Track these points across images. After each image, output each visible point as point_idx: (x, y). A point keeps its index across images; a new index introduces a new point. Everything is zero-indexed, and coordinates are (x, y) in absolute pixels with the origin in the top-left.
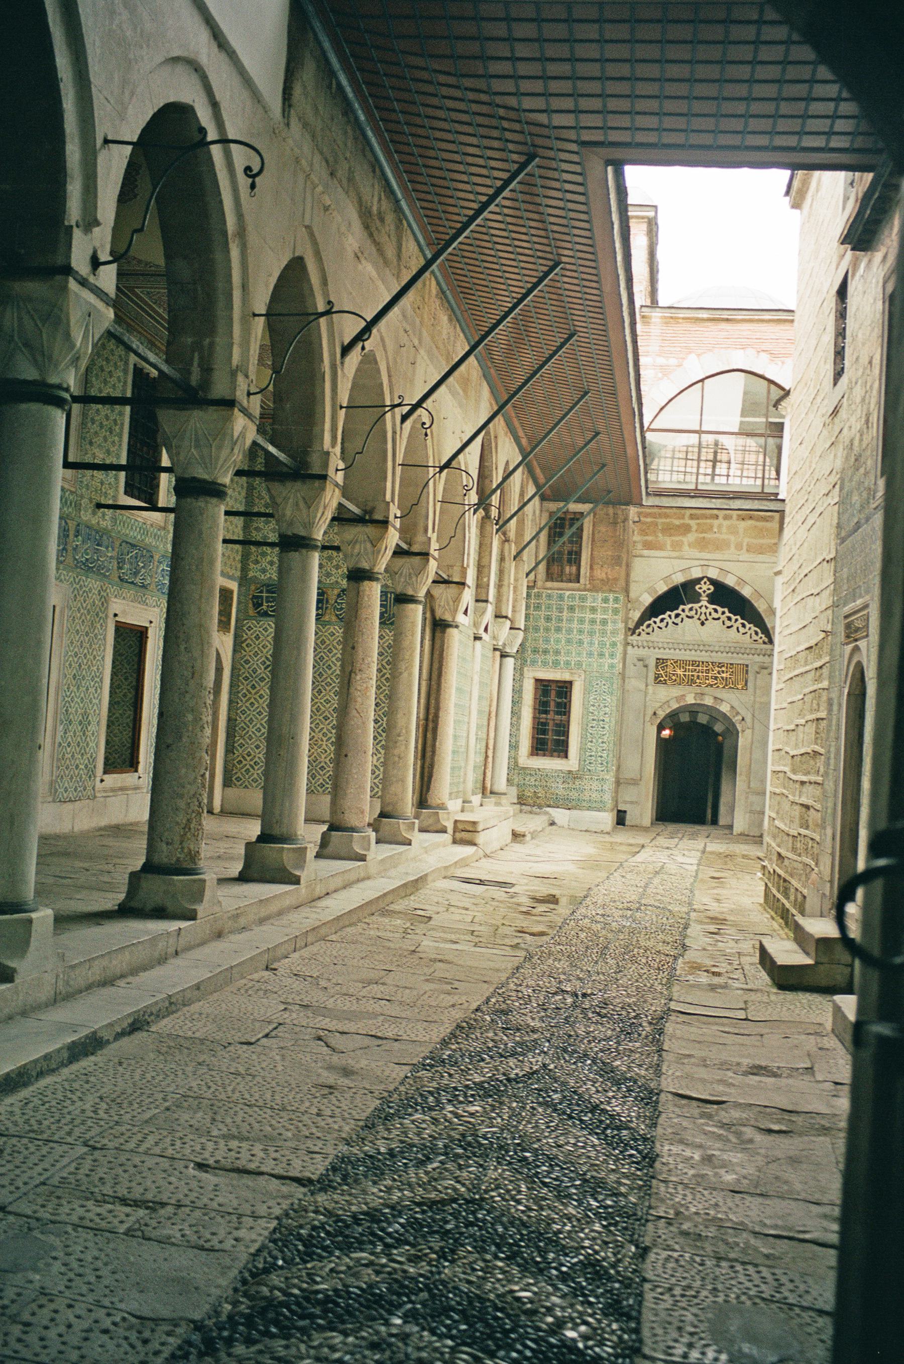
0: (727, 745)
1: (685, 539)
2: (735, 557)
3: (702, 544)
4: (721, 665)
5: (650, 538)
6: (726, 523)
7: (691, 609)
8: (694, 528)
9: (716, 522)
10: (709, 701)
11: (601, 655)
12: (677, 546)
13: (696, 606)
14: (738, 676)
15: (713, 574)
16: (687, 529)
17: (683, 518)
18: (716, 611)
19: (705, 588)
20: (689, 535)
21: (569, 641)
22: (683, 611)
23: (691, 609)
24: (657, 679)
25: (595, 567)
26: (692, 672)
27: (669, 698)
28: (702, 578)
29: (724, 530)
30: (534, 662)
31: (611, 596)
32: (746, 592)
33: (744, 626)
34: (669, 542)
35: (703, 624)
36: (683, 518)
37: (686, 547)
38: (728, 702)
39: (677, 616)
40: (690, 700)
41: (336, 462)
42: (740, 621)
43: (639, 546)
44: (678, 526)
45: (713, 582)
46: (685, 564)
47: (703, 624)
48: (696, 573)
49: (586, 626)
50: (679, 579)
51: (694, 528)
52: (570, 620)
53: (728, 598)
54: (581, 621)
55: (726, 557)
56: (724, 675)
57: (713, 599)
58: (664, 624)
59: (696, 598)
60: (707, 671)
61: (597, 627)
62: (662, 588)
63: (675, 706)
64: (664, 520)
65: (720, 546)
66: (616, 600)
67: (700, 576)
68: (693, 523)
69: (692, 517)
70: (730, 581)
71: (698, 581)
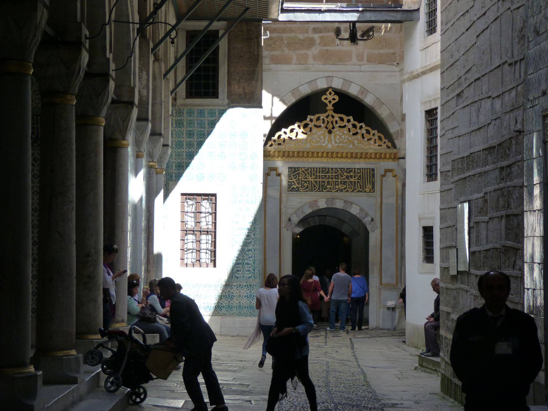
4: (349, 170)
5: (276, 53)
7: (318, 119)
8: (318, 41)
10: (339, 205)
13: (323, 116)
14: (365, 181)
15: (337, 84)
16: (310, 43)
17: (307, 32)
18: (342, 119)
19: (330, 99)
20: (313, 48)
23: (318, 119)
33: (368, 132)
34: (294, 57)
35: (330, 132)
36: (307, 32)
37: (311, 60)
38: (358, 204)
40: (322, 204)
44: (303, 40)
45: (337, 92)
46: (310, 76)
47: (330, 132)
48: (322, 85)
50: (306, 90)
51: (318, 41)
53: (352, 108)
56: (353, 180)
57: (337, 108)
59: (323, 108)
60: (337, 177)
63: (308, 211)
64: (289, 35)
67: (325, 86)
68: (316, 36)
69: (315, 30)
70: (353, 91)
71: (324, 92)
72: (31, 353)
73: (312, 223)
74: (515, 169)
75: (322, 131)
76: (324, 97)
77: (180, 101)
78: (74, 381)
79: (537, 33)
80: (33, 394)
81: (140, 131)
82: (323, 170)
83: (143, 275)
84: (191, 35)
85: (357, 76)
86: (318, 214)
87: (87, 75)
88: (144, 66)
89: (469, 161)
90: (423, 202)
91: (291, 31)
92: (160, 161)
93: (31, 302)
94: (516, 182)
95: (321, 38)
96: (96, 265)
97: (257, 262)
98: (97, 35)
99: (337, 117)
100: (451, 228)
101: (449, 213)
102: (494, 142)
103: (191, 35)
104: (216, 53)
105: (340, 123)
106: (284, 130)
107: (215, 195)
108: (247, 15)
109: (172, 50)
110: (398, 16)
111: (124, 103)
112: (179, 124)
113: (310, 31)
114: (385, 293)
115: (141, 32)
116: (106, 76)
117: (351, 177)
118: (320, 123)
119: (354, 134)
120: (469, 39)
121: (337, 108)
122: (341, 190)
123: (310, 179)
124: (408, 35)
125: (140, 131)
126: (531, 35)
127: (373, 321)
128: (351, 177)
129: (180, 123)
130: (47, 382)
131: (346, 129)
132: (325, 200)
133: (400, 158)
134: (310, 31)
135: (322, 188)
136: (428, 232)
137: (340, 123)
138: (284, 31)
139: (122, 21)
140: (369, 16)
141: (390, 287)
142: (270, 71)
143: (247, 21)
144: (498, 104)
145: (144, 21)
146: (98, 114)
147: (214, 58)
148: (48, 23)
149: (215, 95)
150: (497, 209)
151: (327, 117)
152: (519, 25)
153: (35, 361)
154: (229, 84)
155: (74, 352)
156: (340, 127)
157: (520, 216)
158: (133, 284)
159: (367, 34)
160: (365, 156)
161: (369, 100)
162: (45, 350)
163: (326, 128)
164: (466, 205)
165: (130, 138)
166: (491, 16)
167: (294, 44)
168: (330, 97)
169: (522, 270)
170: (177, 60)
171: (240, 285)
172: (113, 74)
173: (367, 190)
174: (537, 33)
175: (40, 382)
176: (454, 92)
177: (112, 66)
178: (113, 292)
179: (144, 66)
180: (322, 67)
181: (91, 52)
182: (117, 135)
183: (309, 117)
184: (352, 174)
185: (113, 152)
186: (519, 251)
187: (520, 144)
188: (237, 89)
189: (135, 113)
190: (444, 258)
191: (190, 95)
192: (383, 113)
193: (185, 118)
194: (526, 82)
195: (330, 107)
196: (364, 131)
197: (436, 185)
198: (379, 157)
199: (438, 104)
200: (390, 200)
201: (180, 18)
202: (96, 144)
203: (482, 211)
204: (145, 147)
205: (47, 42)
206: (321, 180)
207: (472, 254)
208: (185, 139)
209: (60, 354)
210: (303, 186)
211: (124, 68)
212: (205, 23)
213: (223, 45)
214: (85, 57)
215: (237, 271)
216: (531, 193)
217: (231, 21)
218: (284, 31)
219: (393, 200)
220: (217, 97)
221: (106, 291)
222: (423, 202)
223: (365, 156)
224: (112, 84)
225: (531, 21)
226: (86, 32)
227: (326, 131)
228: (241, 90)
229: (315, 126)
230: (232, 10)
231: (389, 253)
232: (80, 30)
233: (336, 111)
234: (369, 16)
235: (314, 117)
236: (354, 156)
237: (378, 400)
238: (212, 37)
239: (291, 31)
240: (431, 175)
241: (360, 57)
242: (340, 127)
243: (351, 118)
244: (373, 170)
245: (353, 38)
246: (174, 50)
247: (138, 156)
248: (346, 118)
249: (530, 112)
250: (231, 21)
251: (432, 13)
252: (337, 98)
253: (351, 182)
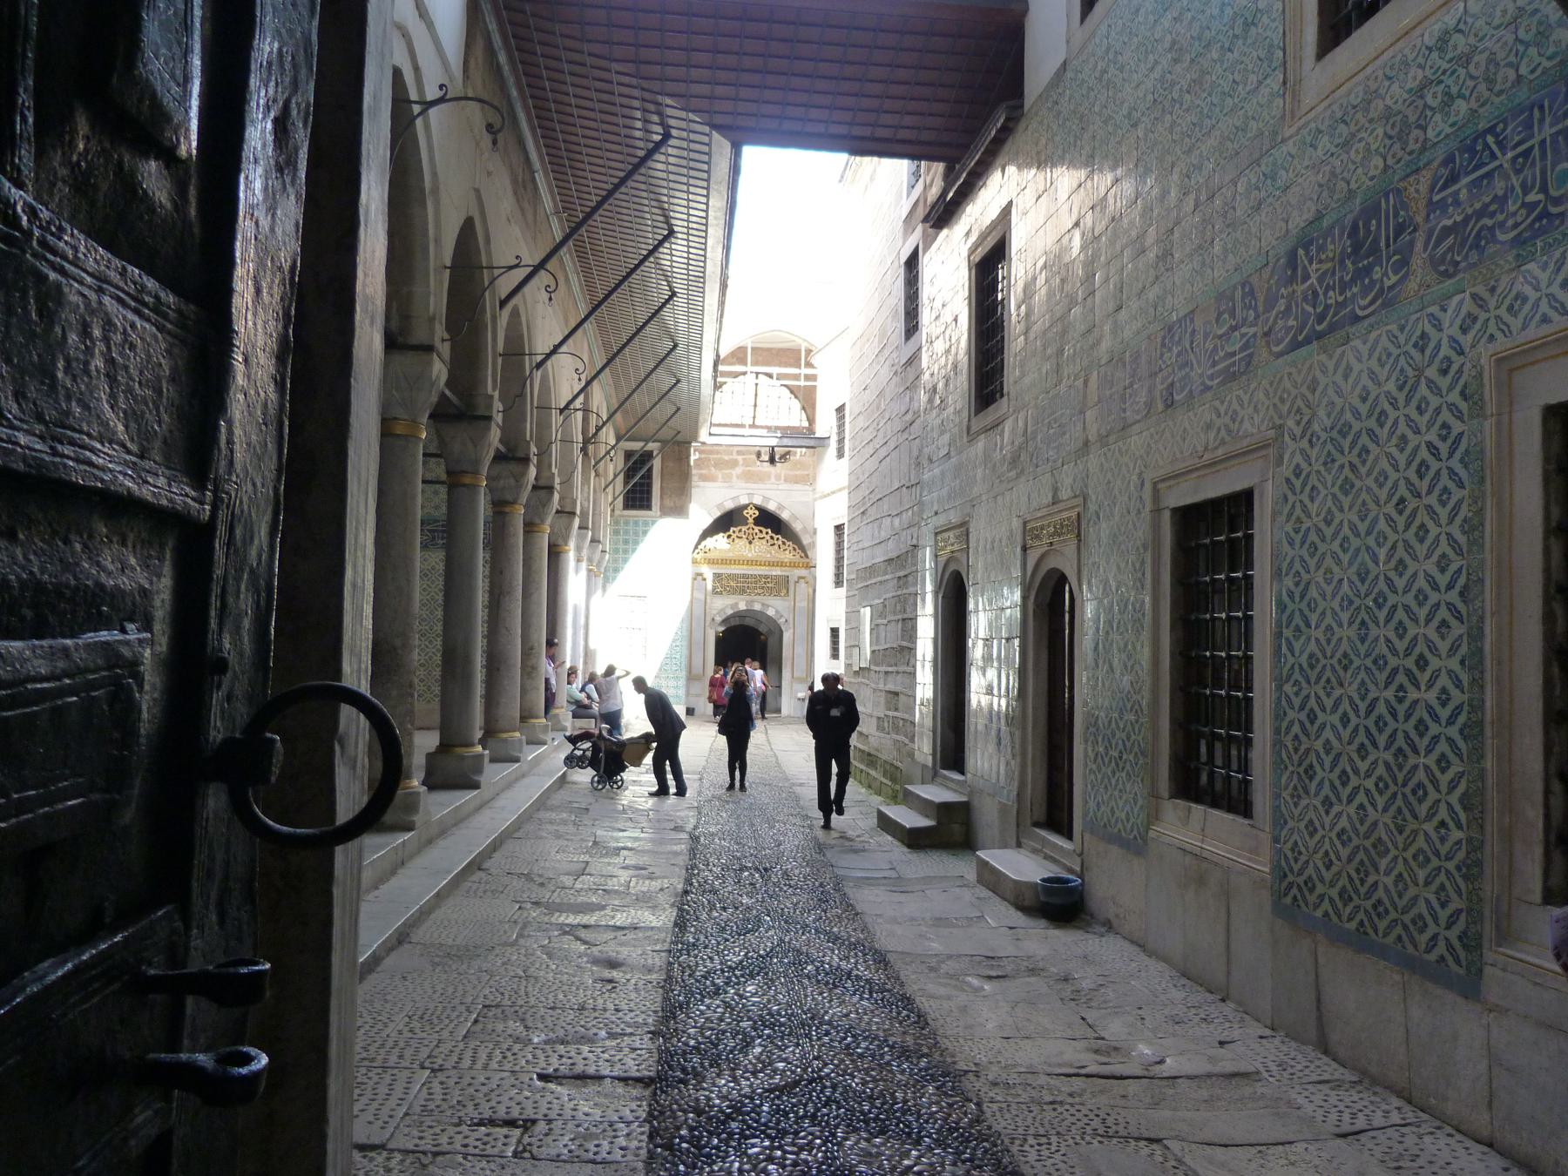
0: (771, 642)
4: (766, 577)
10: (757, 607)
12: (727, 479)
14: (780, 586)
15: (758, 501)
16: (734, 464)
19: (751, 513)
27: (726, 605)
32: (785, 515)
38: (774, 607)
40: (742, 606)
41: (498, 406)
45: (757, 508)
46: (734, 493)
48: (744, 501)
50: (730, 505)
53: (770, 521)
57: (757, 522)
59: (744, 521)
63: (730, 612)
68: (740, 458)
69: (739, 453)
71: (746, 507)
72: (479, 734)
73: (733, 623)
74: (910, 578)
75: (744, 542)
77: (617, 512)
78: (517, 760)
79: (931, 460)
80: (479, 771)
81: (581, 538)
82: (744, 576)
83: (581, 667)
84: (628, 455)
85: (777, 495)
86: (739, 615)
87: (535, 487)
88: (586, 480)
89: (871, 570)
90: (831, 605)
91: (718, 453)
92: (598, 566)
93: (479, 689)
94: (912, 590)
96: (539, 657)
98: (544, 453)
99: (757, 529)
100: (854, 629)
101: (852, 615)
102: (893, 555)
103: (628, 455)
104: (650, 470)
108: (679, 438)
109: (611, 467)
110: (812, 443)
111: (566, 513)
112: (616, 532)
114: (797, 686)
115: (584, 450)
116: (550, 489)
120: (872, 465)
121: (757, 522)
124: (820, 458)
125: (581, 538)
126: (925, 462)
127: (785, 711)
130: (493, 760)
133: (810, 566)
135: (743, 591)
136: (835, 632)
138: (711, 452)
139: (567, 441)
140: (786, 442)
141: (800, 680)
142: (696, 493)
143: (679, 443)
144: (897, 521)
145: (586, 441)
146: (543, 522)
147: (649, 475)
148: (501, 441)
150: (895, 613)
152: (915, 453)
153: (483, 742)
155: (517, 734)
157: (914, 619)
158: (572, 672)
159: (784, 457)
160: (781, 564)
162: (491, 732)
164: (868, 610)
165: (572, 544)
166: (892, 445)
167: (719, 464)
169: (914, 667)
170: (616, 476)
172: (557, 487)
174: (931, 460)
175: (486, 760)
176: (861, 511)
177: (557, 480)
178: (553, 681)
179: (586, 480)
181: (539, 467)
182: (560, 542)
185: (555, 554)
186: (911, 650)
187: (915, 557)
188: (668, 503)
189: (577, 522)
190: (849, 656)
191: (627, 506)
192: (797, 527)
193: (622, 527)
194: (920, 503)
195: (751, 520)
197: (843, 591)
198: (793, 565)
199: (844, 520)
200: (802, 604)
201: (618, 439)
202: (541, 549)
203: (882, 615)
204: (585, 553)
205: (499, 458)
206: (742, 585)
207: (873, 652)
208: (621, 546)
209: (505, 735)
211: (567, 482)
212: (641, 444)
213: (657, 463)
214: (533, 472)
216: (924, 600)
217: (664, 442)
218: (711, 452)
219: (804, 604)
221: (547, 680)
222: (831, 605)
223: (781, 564)
224: (556, 496)
225: (926, 450)
226: (534, 449)
230: (666, 433)
231: (800, 650)
232: (529, 448)
234: (786, 442)
237: (787, 779)
238: (647, 457)
239: (718, 453)
240: (838, 582)
241: (778, 477)
245: (772, 461)
246: (614, 467)
247: (579, 560)
249: (924, 529)
250: (664, 442)
251: (841, 441)
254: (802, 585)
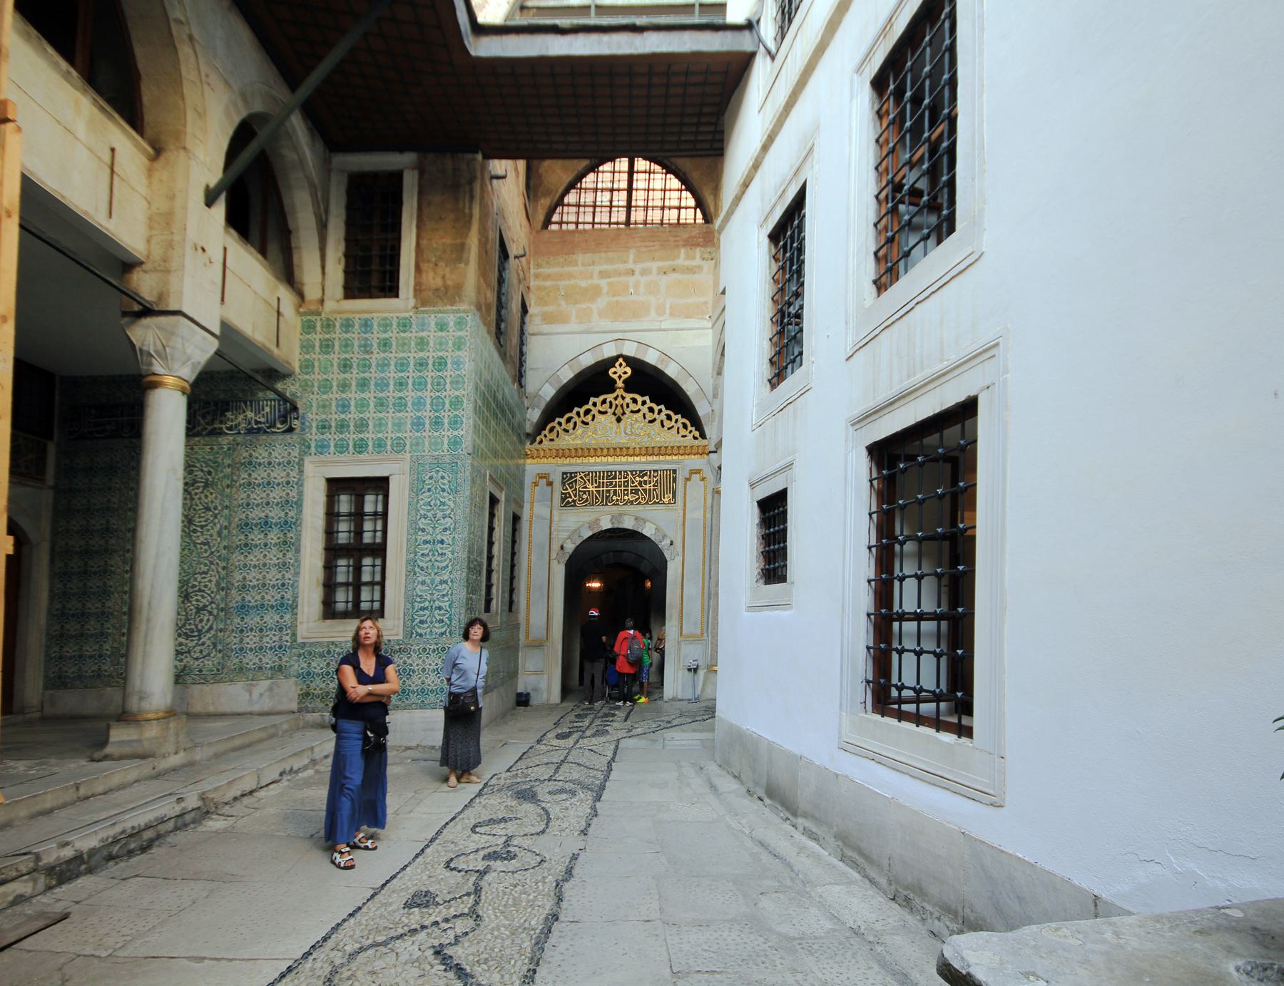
1: (594, 307)
2: (656, 325)
3: (616, 312)
4: (642, 473)
6: (644, 279)
7: (604, 402)
8: (605, 290)
9: (631, 280)
10: (628, 524)
11: (437, 423)
13: (610, 397)
15: (630, 350)
16: (595, 292)
18: (635, 401)
19: (621, 372)
20: (599, 300)
21: (381, 404)
22: (595, 404)
23: (604, 402)
24: (566, 502)
25: (424, 266)
26: (609, 488)
28: (616, 358)
29: (642, 289)
30: (322, 447)
31: (451, 319)
34: (574, 313)
35: (619, 420)
38: (652, 521)
39: (587, 412)
40: (606, 524)
42: (665, 412)
43: (537, 320)
45: (630, 361)
47: (619, 420)
48: (609, 352)
49: (411, 373)
50: (588, 360)
52: (384, 365)
54: (402, 366)
55: (645, 326)
56: (647, 487)
57: (630, 386)
58: (571, 425)
59: (610, 386)
60: (626, 484)
61: (430, 374)
62: (567, 375)
63: (588, 534)
64: (567, 282)
65: (638, 311)
66: (460, 324)
67: (614, 354)
68: (603, 283)
71: (611, 362)
76: (612, 370)
82: (610, 475)
95: (610, 284)
97: (456, 605)
99: (628, 396)
105: (633, 407)
106: (558, 419)
107: (385, 480)
113: (596, 275)
117: (645, 482)
118: (605, 407)
119: (650, 422)
121: (630, 386)
122: (632, 503)
123: (591, 488)
128: (645, 482)
129: (328, 346)
131: (641, 414)
132: (609, 517)
134: (596, 275)
135: (606, 500)
137: (633, 407)
149: (391, 290)
151: (616, 399)
154: (418, 269)
156: (632, 412)
161: (671, 371)
163: (614, 414)
168: (620, 371)
171: (425, 649)
173: (666, 500)
180: (606, 324)
183: (592, 400)
184: (646, 478)
195: (620, 384)
196: (663, 416)
210: (581, 499)
215: (422, 622)
220: (397, 296)
227: (614, 418)
228: (439, 282)
229: (600, 412)
233: (627, 390)
235: (599, 400)
236: (648, 452)
242: (632, 412)
243: (647, 398)
244: (675, 471)
248: (640, 399)
252: (629, 370)
253: (645, 490)
254: (696, 484)
